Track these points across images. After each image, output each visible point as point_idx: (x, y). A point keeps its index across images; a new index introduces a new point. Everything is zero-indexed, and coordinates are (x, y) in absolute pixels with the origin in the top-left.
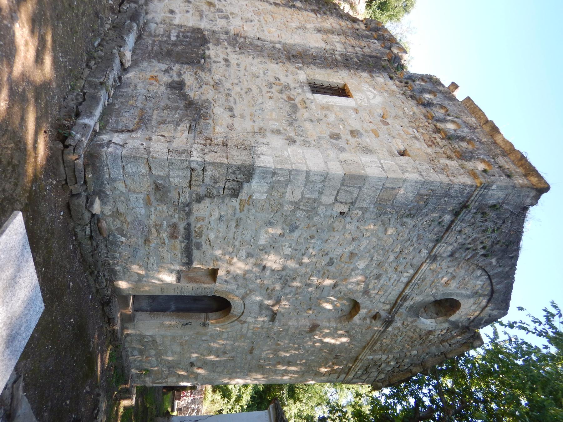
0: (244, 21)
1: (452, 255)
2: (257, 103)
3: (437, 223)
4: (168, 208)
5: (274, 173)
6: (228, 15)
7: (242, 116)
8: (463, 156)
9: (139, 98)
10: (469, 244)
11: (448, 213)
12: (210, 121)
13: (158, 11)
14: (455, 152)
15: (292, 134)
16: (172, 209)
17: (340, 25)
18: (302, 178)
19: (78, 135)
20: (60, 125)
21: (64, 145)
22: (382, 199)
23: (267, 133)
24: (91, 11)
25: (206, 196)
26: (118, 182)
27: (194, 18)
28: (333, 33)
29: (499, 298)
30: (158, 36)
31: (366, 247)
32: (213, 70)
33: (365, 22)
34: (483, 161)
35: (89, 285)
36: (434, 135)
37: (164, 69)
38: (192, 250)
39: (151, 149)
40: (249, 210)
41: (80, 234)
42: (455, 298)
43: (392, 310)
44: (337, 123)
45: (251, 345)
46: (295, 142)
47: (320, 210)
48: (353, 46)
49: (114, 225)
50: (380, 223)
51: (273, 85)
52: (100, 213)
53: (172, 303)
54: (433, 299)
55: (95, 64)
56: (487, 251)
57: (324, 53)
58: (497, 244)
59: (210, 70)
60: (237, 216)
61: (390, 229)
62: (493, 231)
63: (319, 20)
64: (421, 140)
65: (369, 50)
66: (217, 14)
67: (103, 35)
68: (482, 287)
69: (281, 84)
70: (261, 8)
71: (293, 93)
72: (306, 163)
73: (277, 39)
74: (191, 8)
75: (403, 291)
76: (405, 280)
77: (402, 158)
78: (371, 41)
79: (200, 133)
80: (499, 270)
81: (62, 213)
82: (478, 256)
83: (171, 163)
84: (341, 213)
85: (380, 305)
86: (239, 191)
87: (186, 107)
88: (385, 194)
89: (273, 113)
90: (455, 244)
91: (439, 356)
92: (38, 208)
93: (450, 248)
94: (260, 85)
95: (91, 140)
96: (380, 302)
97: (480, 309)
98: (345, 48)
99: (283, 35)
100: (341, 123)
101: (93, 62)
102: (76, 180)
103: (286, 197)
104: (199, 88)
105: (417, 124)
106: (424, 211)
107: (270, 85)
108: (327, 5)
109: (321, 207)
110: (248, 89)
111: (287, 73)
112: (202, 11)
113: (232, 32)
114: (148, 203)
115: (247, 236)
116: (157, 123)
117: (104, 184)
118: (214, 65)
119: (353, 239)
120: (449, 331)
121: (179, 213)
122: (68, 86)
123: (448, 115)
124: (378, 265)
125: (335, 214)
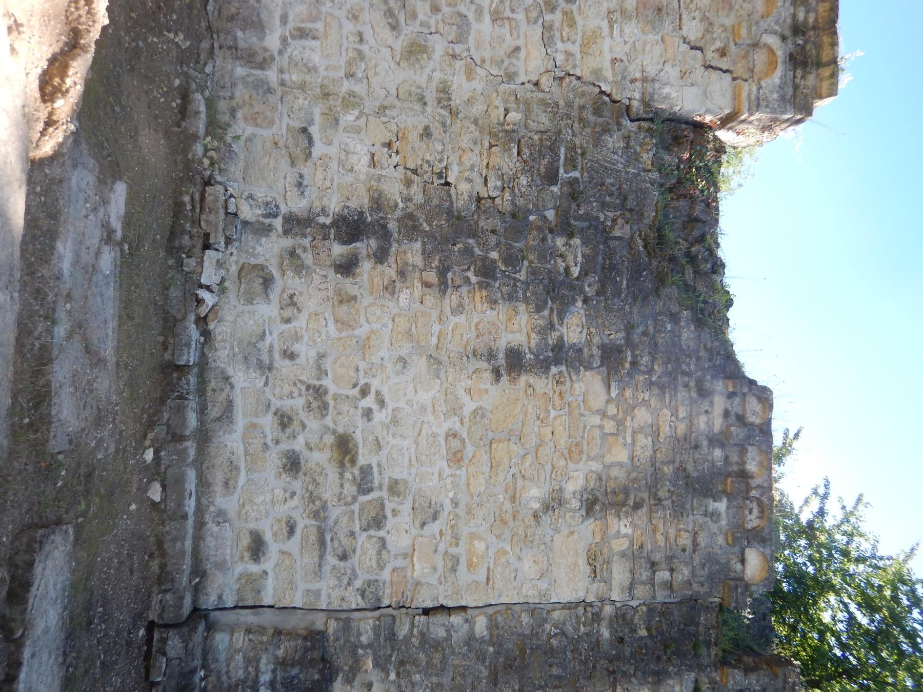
0: (417, 524)
6: (383, 506)
17: (656, 434)
48: (653, 564)
57: (578, 623)
66: (356, 507)
78: (713, 505)
98: (631, 587)
113: (386, 602)
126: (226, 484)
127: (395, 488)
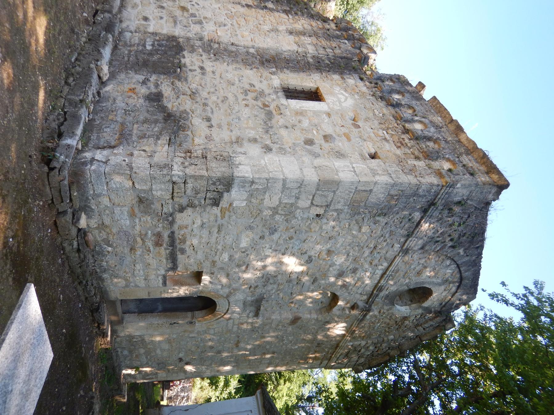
0: (217, 26)
1: (422, 248)
2: (234, 112)
3: (407, 220)
4: (152, 218)
5: (253, 182)
6: (201, 20)
7: (220, 126)
8: (429, 156)
9: (119, 112)
10: (438, 237)
11: (417, 211)
12: (189, 133)
13: (132, 18)
14: (422, 152)
15: (268, 142)
16: (156, 220)
18: (279, 186)
19: (62, 157)
20: (43, 148)
21: (49, 167)
22: (355, 201)
23: (244, 142)
24: (66, 28)
25: (188, 206)
26: (102, 197)
27: (168, 24)
28: (304, 34)
29: (468, 284)
30: (134, 45)
31: (342, 245)
32: (190, 79)
33: (335, 21)
34: (448, 160)
35: (78, 294)
36: (403, 136)
37: (141, 81)
38: (177, 255)
39: (133, 165)
40: (230, 217)
41: (68, 248)
42: (427, 286)
43: (369, 300)
44: (312, 127)
45: (237, 339)
46: (271, 150)
47: (298, 213)
48: (324, 48)
49: (100, 237)
50: (355, 222)
51: (248, 92)
52: (86, 227)
53: (159, 304)
54: (406, 288)
55: (74, 80)
56: (455, 243)
57: (296, 56)
58: (463, 236)
59: (186, 80)
60: (218, 222)
61: (364, 227)
62: (460, 225)
63: (291, 21)
64: (391, 141)
65: (340, 51)
66: (190, 19)
67: (79, 49)
68: (452, 275)
69: (256, 91)
70: (233, 10)
71: (268, 99)
72: (282, 170)
73: (250, 44)
74: (164, 13)
75: (379, 282)
76: (379, 272)
77: (373, 160)
78: (342, 41)
79: (180, 145)
80: (467, 259)
81: (50, 230)
82: (447, 247)
83: (153, 178)
84: (317, 215)
85: (358, 296)
86: (220, 200)
87: (165, 120)
88: (357, 196)
89: (249, 121)
90: (425, 238)
91: (414, 339)
92: (27, 231)
93: (420, 242)
94: (235, 92)
95: (75, 158)
96: (357, 293)
97: (451, 295)
98: (317, 50)
99: (256, 39)
100: (315, 128)
101: (72, 79)
102: (62, 199)
103: (265, 203)
104: (177, 99)
105: (387, 125)
106: (395, 210)
107: (246, 92)
108: (299, 5)
109: (298, 211)
110: (224, 97)
111: (261, 79)
112: (176, 16)
113: (206, 38)
114: (132, 215)
115: (229, 240)
116: (138, 137)
117: (88, 199)
118: (190, 74)
119: (330, 238)
120: (423, 316)
121: (163, 222)
122: (49, 107)
123: (416, 115)
124: (355, 260)
125: (311, 216)
126: (133, 7)
127: (205, 18)
